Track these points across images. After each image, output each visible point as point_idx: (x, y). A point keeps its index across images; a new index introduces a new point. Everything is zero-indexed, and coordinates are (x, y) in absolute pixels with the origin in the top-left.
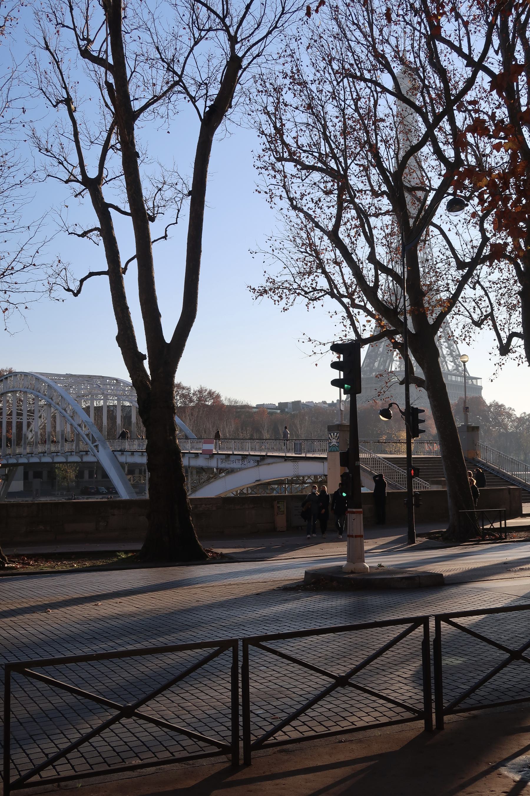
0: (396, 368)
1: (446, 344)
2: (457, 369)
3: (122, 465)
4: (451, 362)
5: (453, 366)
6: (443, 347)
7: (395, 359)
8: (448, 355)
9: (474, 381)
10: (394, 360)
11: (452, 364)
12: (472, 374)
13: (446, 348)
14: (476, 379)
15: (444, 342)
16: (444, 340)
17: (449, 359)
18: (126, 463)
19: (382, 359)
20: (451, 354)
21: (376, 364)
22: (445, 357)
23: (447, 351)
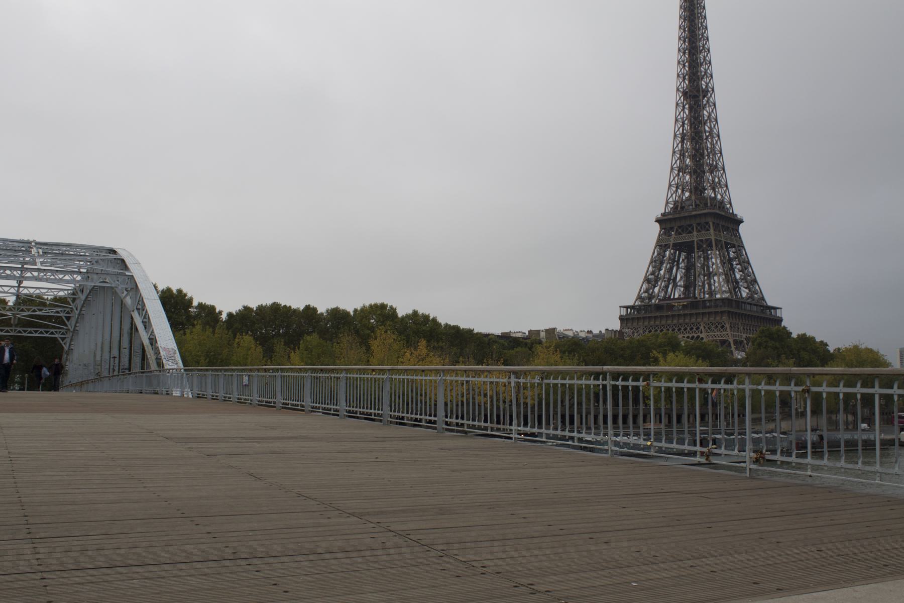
1: (739, 266)
2: (751, 297)
4: (746, 288)
5: (748, 294)
6: (736, 270)
8: (742, 279)
9: (773, 311)
10: (677, 286)
11: (747, 291)
12: (770, 302)
13: (740, 271)
14: (775, 308)
15: (737, 264)
16: (737, 262)
19: (663, 283)
21: (656, 290)
23: (741, 276)
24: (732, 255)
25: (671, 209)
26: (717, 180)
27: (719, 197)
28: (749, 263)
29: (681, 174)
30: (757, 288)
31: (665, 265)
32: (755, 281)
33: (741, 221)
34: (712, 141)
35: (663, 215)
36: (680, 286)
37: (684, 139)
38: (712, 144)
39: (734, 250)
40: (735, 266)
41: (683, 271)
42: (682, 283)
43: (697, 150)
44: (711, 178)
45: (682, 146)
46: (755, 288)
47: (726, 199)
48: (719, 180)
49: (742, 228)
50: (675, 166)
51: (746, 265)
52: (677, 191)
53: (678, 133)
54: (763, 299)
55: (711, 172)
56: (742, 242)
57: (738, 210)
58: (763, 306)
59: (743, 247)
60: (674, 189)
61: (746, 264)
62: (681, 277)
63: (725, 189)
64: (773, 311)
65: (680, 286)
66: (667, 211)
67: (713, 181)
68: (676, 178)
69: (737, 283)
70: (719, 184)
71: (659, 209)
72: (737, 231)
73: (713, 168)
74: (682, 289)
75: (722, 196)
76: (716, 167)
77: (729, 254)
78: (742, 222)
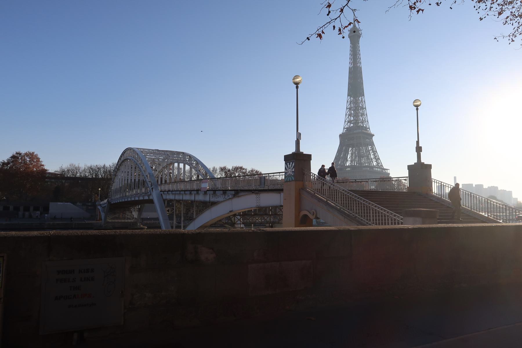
0: (349, 164)
1: (372, 153)
2: (378, 165)
3: (164, 200)
5: (376, 164)
7: (348, 160)
9: (386, 171)
11: (376, 163)
13: (373, 155)
14: (387, 169)
16: (372, 152)
17: (374, 160)
18: (175, 200)
19: (342, 160)
20: (375, 158)
21: (340, 162)
22: (372, 159)
24: (370, 149)
25: (346, 131)
26: (364, 119)
27: (365, 126)
28: (376, 152)
29: (350, 117)
30: (380, 161)
31: (343, 153)
32: (379, 159)
33: (374, 135)
34: (362, 103)
35: (343, 133)
36: (349, 161)
37: (351, 103)
38: (362, 105)
39: (370, 146)
40: (371, 153)
41: (350, 155)
42: (350, 160)
43: (356, 107)
44: (361, 118)
45: (350, 105)
46: (379, 162)
47: (368, 127)
48: (365, 119)
49: (374, 138)
50: (347, 114)
51: (376, 152)
52: (348, 123)
53: (349, 101)
54: (382, 166)
55: (361, 116)
56: (374, 144)
57: (372, 131)
58: (382, 168)
59: (374, 145)
60: (347, 123)
61: (375, 152)
62: (349, 157)
63: (367, 122)
64: (386, 171)
65: (349, 161)
66: (344, 132)
67: (363, 120)
68: (348, 119)
69: (372, 159)
70: (365, 121)
71: (341, 131)
72: (372, 139)
73: (363, 115)
74: (350, 162)
75: (366, 125)
76: (364, 114)
77: (368, 148)
78: (374, 135)
